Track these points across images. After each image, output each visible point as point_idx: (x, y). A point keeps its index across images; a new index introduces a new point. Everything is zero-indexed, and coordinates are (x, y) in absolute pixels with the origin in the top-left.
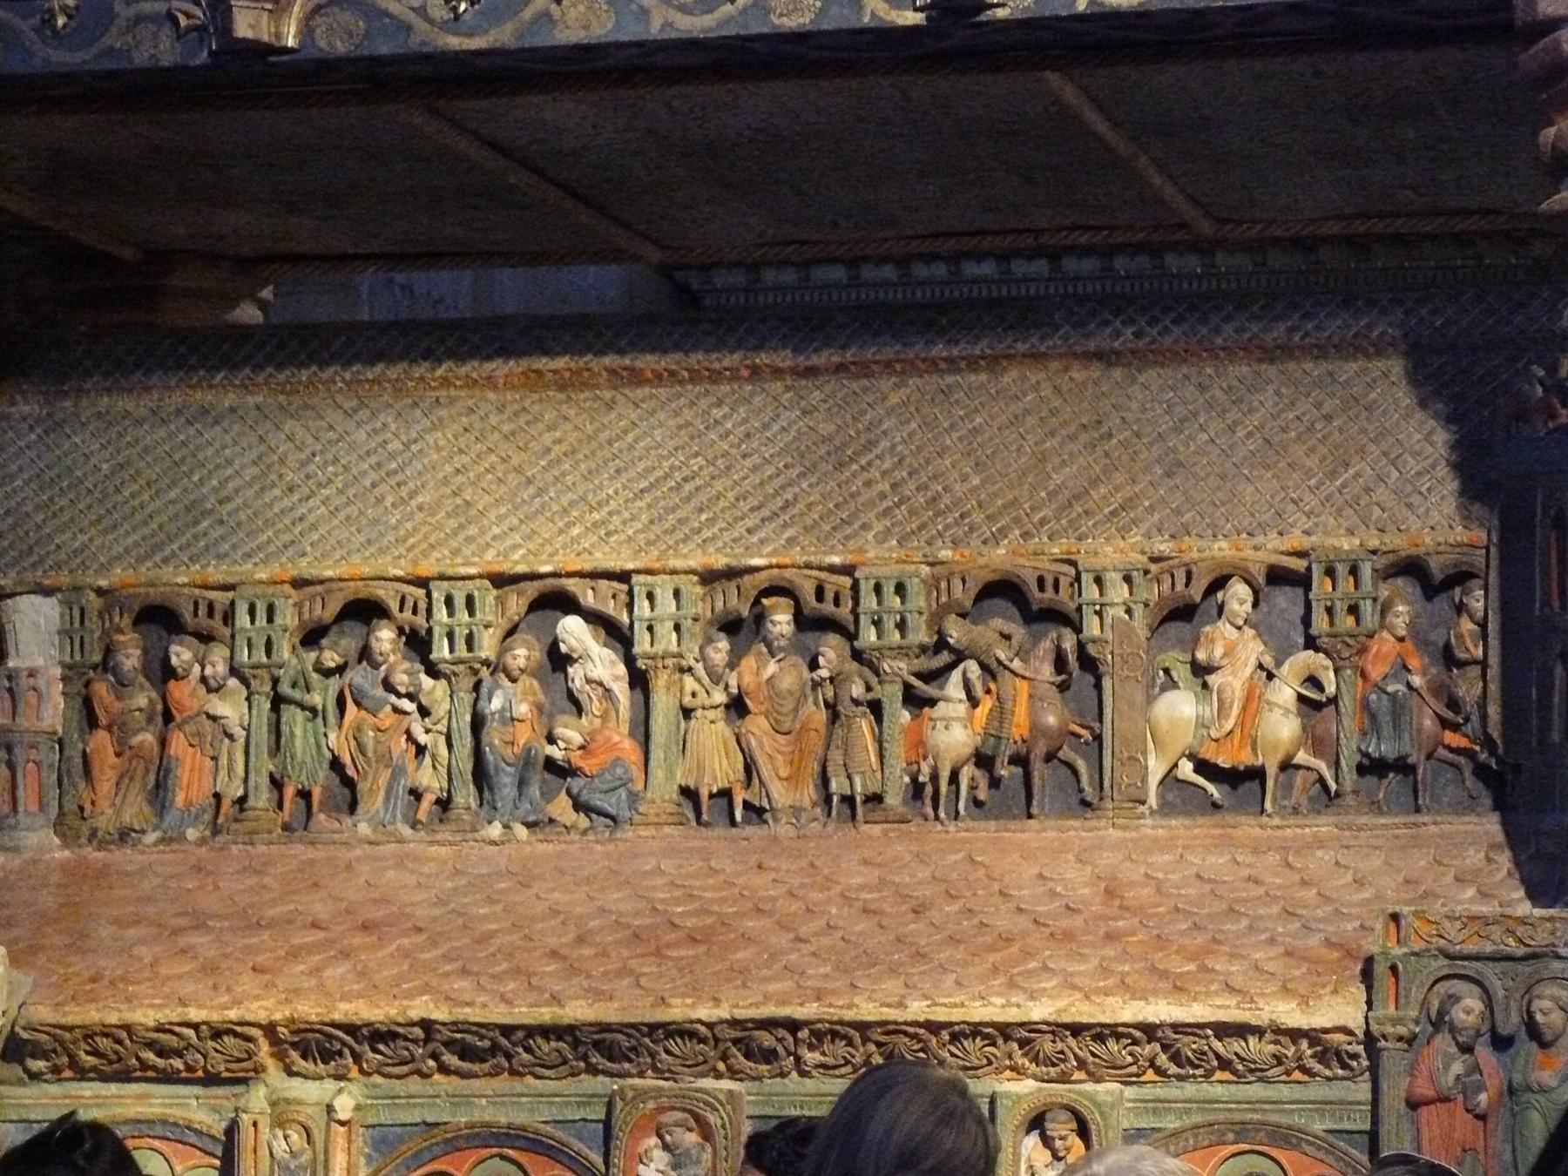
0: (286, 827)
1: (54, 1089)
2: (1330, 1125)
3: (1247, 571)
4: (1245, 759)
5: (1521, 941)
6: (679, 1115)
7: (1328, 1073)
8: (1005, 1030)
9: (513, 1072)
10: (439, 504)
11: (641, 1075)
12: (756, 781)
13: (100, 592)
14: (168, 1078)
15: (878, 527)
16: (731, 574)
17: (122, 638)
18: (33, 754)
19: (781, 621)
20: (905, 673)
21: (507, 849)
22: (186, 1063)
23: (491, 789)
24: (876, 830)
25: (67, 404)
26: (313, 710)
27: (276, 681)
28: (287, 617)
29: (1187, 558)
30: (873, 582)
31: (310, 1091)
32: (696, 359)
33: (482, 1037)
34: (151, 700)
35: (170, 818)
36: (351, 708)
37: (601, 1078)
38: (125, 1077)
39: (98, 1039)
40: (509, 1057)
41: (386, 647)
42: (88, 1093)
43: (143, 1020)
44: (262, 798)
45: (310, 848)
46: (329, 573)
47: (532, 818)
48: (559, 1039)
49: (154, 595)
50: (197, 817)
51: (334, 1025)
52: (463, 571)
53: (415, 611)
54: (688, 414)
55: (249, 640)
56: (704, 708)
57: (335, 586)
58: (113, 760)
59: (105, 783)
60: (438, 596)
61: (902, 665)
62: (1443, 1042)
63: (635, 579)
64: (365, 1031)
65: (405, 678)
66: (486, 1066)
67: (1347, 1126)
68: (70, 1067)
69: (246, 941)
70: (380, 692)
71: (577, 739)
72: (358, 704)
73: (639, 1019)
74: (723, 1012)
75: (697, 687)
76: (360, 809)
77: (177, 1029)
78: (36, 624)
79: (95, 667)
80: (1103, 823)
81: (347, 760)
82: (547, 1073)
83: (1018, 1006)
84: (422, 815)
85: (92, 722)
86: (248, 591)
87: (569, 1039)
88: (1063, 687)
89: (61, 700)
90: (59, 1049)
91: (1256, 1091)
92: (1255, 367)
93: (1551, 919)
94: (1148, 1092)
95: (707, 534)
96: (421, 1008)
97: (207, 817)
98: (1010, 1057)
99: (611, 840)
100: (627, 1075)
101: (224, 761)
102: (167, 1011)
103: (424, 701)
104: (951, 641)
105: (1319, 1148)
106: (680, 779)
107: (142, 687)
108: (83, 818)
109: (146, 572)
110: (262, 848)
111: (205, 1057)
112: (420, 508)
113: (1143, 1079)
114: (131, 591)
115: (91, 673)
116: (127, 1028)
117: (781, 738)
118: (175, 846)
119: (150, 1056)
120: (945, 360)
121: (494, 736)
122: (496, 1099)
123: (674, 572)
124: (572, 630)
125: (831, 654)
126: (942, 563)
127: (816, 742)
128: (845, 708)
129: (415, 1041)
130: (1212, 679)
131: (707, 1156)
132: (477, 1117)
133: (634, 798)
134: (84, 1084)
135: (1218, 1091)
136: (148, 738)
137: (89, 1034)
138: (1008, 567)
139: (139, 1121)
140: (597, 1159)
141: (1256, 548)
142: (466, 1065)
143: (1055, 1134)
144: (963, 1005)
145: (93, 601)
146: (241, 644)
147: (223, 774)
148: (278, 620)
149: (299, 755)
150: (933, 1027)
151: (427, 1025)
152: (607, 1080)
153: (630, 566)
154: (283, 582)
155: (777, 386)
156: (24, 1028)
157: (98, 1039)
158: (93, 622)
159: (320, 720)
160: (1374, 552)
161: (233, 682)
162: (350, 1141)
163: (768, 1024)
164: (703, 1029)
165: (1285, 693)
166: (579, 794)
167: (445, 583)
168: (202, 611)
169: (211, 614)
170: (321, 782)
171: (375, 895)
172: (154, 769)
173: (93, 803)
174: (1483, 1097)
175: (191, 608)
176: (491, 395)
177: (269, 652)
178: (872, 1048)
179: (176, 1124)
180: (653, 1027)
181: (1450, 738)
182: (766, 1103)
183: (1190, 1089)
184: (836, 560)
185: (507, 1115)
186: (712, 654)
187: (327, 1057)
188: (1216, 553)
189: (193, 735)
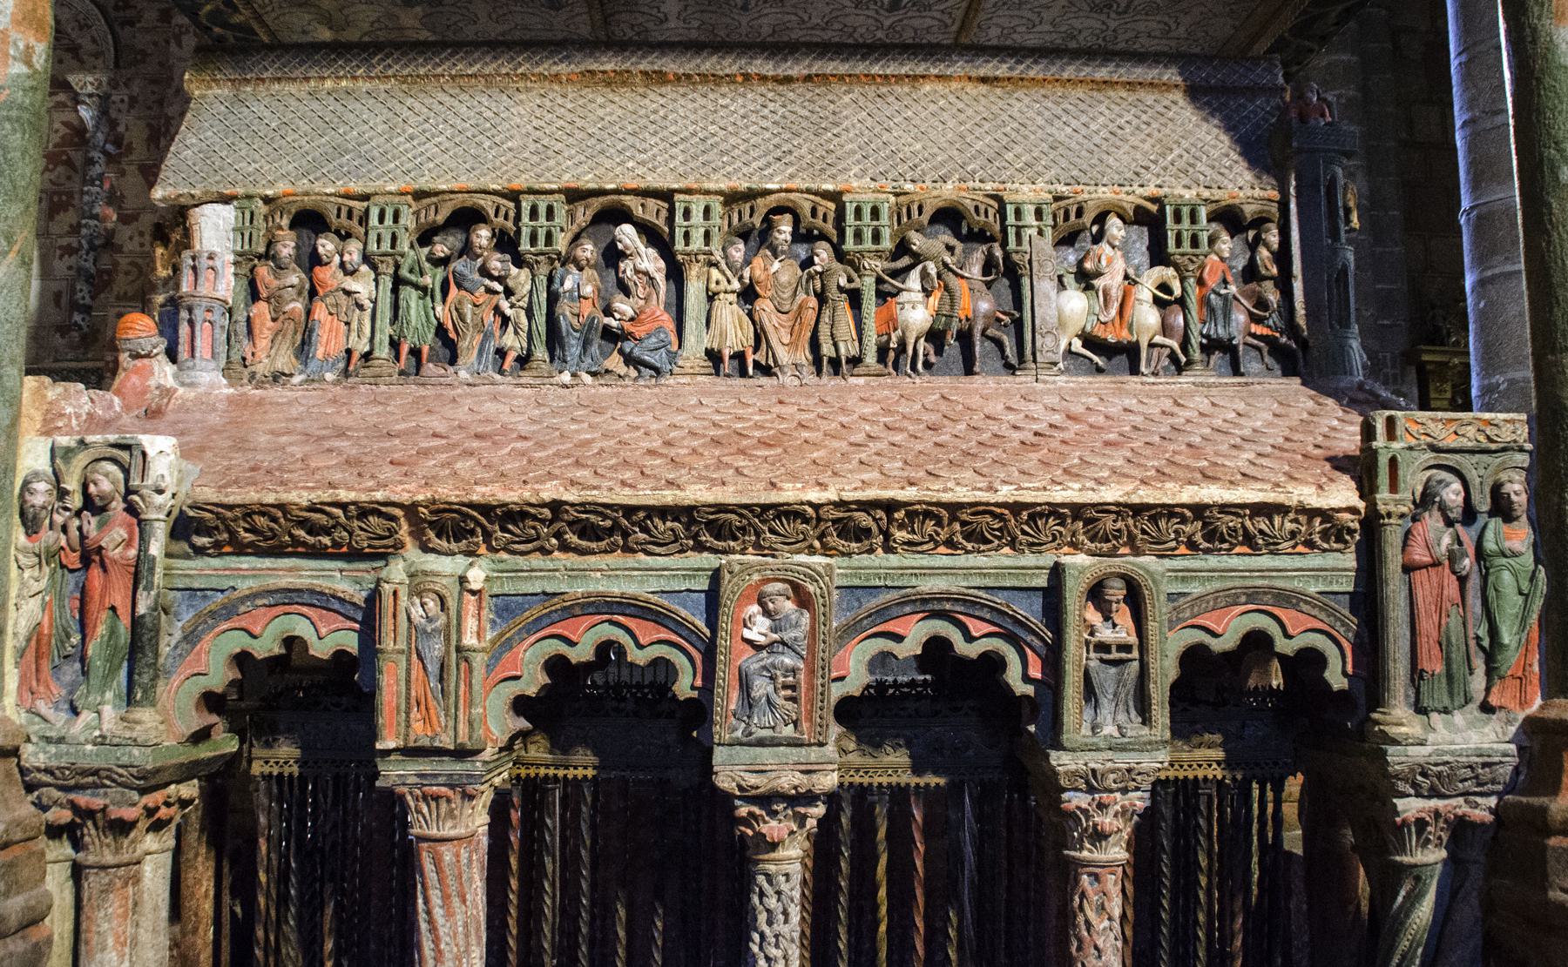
0: (402, 373)
1: (216, 562)
2: (1322, 588)
3: (1122, 208)
4: (1125, 336)
5: (1488, 438)
6: (779, 586)
7: (1326, 546)
8: (1077, 510)
9: (627, 549)
10: (525, 147)
11: (743, 552)
12: (764, 346)
13: (267, 200)
14: (317, 553)
15: (856, 169)
16: (751, 195)
17: (281, 233)
18: (209, 316)
19: (785, 229)
20: (879, 269)
21: (576, 391)
22: (333, 540)
23: (563, 348)
24: (861, 381)
25: (248, 89)
26: (424, 289)
27: (397, 267)
28: (407, 219)
29: (1080, 198)
30: (855, 205)
31: (446, 566)
33: (605, 517)
34: (301, 280)
35: (313, 366)
36: (453, 291)
37: (705, 554)
38: (277, 552)
40: (626, 534)
41: (484, 242)
42: (245, 566)
43: (297, 500)
44: (383, 351)
45: (421, 389)
46: (444, 187)
47: (593, 369)
48: (676, 519)
50: (333, 365)
51: (471, 505)
52: (547, 186)
53: (506, 218)
55: (379, 235)
56: (726, 292)
57: (446, 197)
58: (270, 324)
59: (263, 343)
60: (526, 206)
61: (878, 263)
62: (1433, 521)
63: (678, 197)
64: (499, 511)
65: (499, 265)
66: (603, 544)
67: (1335, 588)
68: (230, 543)
69: (382, 445)
70: (476, 276)
71: (630, 313)
72: (459, 286)
73: (755, 501)
74: (831, 495)
75: (721, 277)
76: (460, 361)
77: (328, 509)
78: (216, 226)
79: (260, 257)
80: (1029, 379)
81: (450, 326)
82: (658, 550)
83: (1093, 490)
84: (506, 366)
85: (254, 296)
86: (380, 200)
87: (684, 519)
88: (989, 285)
89: (232, 278)
90: (221, 527)
91: (1265, 561)
92: (1090, 93)
93: (1512, 421)
94: (1178, 563)
95: (729, 169)
96: (549, 492)
97: (341, 365)
98: (1074, 535)
99: (655, 386)
100: (733, 552)
101: (354, 325)
102: (320, 493)
103: (510, 283)
104: (914, 248)
105: (1315, 606)
106: (706, 343)
107: (294, 271)
108: (246, 366)
109: (303, 185)
110: (383, 388)
111: (351, 534)
112: (510, 150)
113: (1176, 552)
114: (291, 198)
115: (256, 261)
116: (281, 506)
117: (784, 317)
118: (316, 385)
119: (301, 533)
120: (880, 76)
121: (565, 309)
122: (610, 573)
123: (707, 192)
124: (627, 234)
125: (824, 255)
126: (906, 194)
127: (810, 316)
128: (833, 293)
129: (542, 521)
130: (1096, 282)
131: (806, 618)
132: (591, 589)
133: (672, 357)
134: (243, 559)
135: (1234, 562)
136: (298, 306)
137: (248, 511)
138: (954, 197)
139: (290, 590)
140: (701, 624)
141: (1128, 193)
142: (584, 543)
143: (1114, 598)
144: (1045, 489)
145: (261, 208)
146: (373, 237)
147: (354, 335)
148: (402, 221)
149: (413, 323)
150: (1016, 508)
151: (556, 506)
152: (712, 556)
153: (676, 186)
154: (408, 193)
155: (762, 89)
156: (191, 507)
157: (256, 517)
158: (260, 222)
159: (428, 298)
160: (1206, 200)
161: (364, 268)
162: (480, 608)
164: (809, 510)
165: (1145, 292)
166: (631, 352)
167: (532, 197)
168: (344, 214)
169: (350, 216)
170: (428, 342)
171: (480, 417)
172: (301, 330)
173: (253, 354)
174: (1467, 562)
175: (335, 212)
176: (556, 87)
177: (393, 246)
178: (957, 526)
179: (322, 593)
180: (766, 508)
181: (1254, 328)
182: (855, 575)
183: (1213, 561)
184: (829, 187)
185: (619, 586)
186: (734, 253)
187: (459, 534)
188: (1101, 195)
189: (332, 305)
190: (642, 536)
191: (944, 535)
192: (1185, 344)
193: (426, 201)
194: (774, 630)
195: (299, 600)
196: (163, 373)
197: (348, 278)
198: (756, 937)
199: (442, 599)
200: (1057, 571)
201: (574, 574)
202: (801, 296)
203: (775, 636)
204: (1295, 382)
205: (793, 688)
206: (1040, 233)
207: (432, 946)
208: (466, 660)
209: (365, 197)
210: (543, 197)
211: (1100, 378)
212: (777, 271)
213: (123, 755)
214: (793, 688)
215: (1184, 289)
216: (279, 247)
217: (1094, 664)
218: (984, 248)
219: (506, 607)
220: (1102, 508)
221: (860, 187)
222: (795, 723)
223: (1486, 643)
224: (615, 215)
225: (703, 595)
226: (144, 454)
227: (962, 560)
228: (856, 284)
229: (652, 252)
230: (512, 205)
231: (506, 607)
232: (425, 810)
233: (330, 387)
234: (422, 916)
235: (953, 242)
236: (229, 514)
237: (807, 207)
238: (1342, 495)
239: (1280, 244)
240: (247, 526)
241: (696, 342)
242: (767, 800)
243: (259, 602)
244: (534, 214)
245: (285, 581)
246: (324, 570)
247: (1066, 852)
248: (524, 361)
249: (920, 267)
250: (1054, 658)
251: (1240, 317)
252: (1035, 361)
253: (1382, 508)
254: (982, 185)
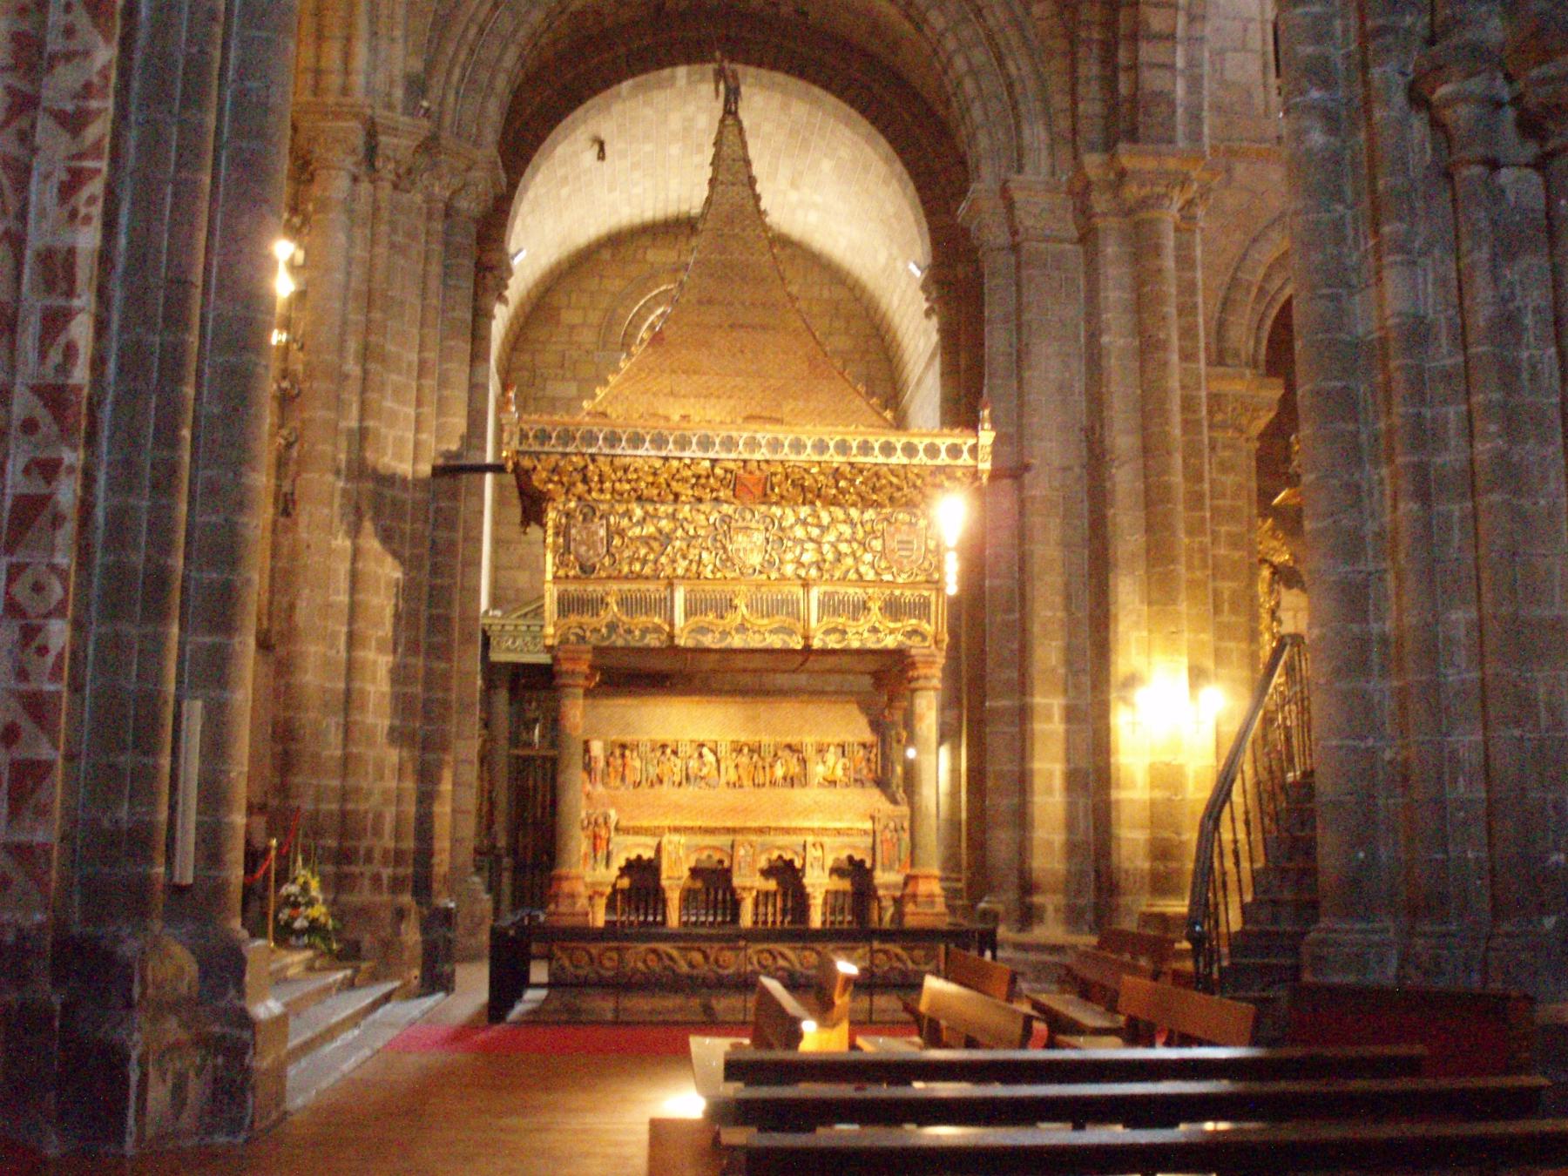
19: (746, 750)
31: (676, 838)
196: (589, 787)
212: (744, 760)
219: (688, 848)
221: (766, 739)
224: (702, 745)
231: (688, 848)
238: (868, 825)
241: (723, 780)
242: (744, 889)
248: (680, 784)
251: (865, 771)
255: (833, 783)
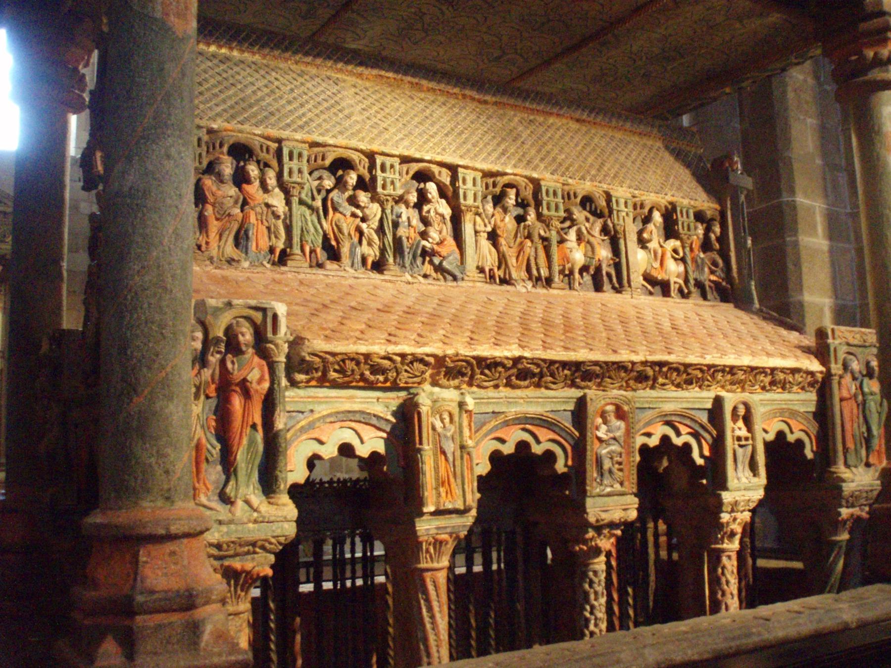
9: (538, 385)
12: (503, 266)
13: (210, 131)
14: (370, 386)
15: (542, 166)
19: (511, 200)
24: (555, 292)
31: (449, 395)
32: (442, 86)
37: (573, 390)
39: (347, 362)
42: (321, 395)
46: (331, 142)
49: (242, 138)
53: (364, 167)
54: (444, 109)
57: (330, 148)
58: (216, 223)
71: (438, 240)
72: (335, 209)
91: (786, 396)
103: (367, 211)
104: (575, 217)
114: (230, 133)
116: (367, 356)
122: (528, 400)
123: (475, 169)
126: (568, 185)
132: (518, 409)
136: (237, 211)
139: (349, 412)
145: (205, 138)
150: (709, 367)
151: (517, 360)
153: (461, 163)
154: (308, 142)
156: (309, 354)
161: (277, 190)
163: (654, 364)
167: (382, 158)
176: (360, 82)
184: (535, 175)
190: (550, 379)
191: (678, 380)
192: (686, 281)
193: (316, 150)
194: (609, 431)
195: (353, 418)
197: (266, 196)
198: (588, 607)
199: (451, 415)
200: (718, 402)
201: (510, 402)
202: (519, 240)
203: (611, 435)
204: (730, 306)
205: (620, 463)
206: (627, 214)
207: (435, 638)
208: (469, 454)
209: (279, 141)
210: (388, 158)
211: (651, 298)
213: (277, 528)
214: (620, 463)
215: (684, 253)
216: (223, 167)
217: (736, 447)
218: (601, 220)
220: (740, 368)
222: (622, 484)
223: (866, 435)
225: (570, 413)
226: (275, 317)
227: (681, 393)
228: (547, 235)
229: (443, 201)
230: (367, 160)
232: (432, 550)
233: (269, 273)
234: (427, 620)
235: (589, 215)
236: (331, 359)
237: (524, 184)
239: (721, 233)
240: (337, 367)
241: (471, 262)
242: (599, 529)
243: (328, 420)
244: (383, 169)
245: (347, 407)
246: (369, 398)
247: (713, 546)
249: (575, 228)
250: (718, 445)
252: (630, 286)
253: (833, 371)
254: (600, 185)
255: (664, 288)
